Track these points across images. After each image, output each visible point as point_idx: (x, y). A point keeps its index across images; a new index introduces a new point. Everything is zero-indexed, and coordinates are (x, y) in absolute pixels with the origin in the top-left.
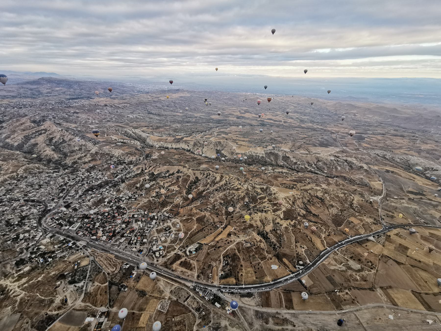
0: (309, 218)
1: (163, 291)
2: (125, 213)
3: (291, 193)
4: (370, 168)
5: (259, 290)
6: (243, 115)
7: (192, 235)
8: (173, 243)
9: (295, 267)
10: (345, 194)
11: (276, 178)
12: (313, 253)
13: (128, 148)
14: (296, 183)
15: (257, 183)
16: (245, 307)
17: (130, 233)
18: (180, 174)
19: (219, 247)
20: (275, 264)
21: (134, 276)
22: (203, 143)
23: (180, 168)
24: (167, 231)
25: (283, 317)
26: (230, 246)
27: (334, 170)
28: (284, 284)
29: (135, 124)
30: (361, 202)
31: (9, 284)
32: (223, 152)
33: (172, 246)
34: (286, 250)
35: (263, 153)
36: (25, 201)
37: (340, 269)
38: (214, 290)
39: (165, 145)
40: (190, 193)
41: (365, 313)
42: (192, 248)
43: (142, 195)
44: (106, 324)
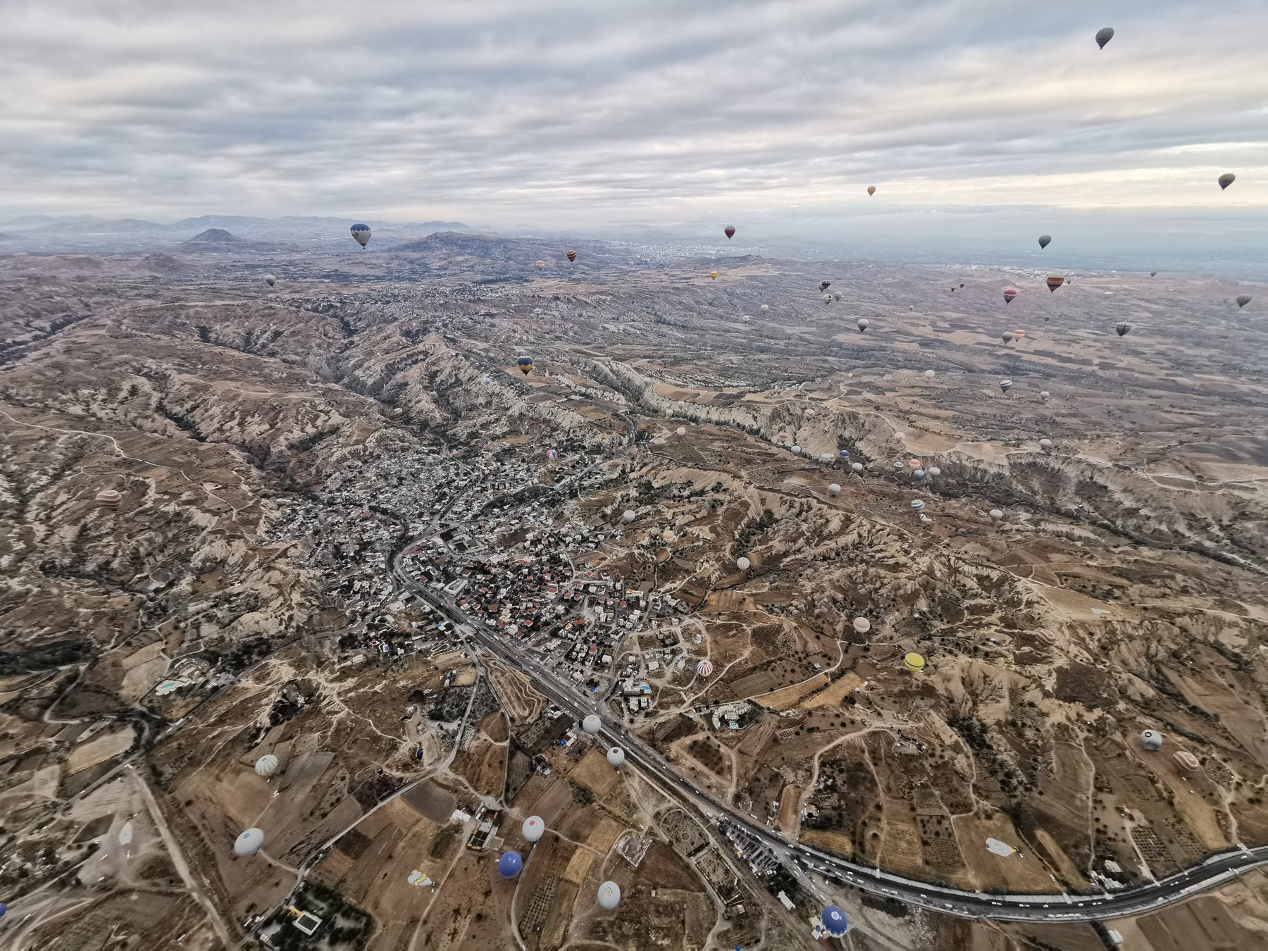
0: (1169, 717)
1: (635, 807)
2: (569, 578)
3: (1098, 612)
5: (930, 902)
6: (943, 336)
7: (738, 675)
8: (680, 684)
9: (1086, 876)
11: (1042, 550)
12: (1174, 849)
13: (594, 410)
14: (1125, 582)
15: (966, 556)
16: (875, 941)
17: (574, 630)
18: (721, 496)
19: (811, 730)
20: (1005, 840)
21: (569, 743)
22: (799, 412)
23: (725, 477)
24: (666, 646)
28: (1033, 918)
29: (619, 349)
31: (322, 681)
32: (860, 445)
33: (676, 692)
34: (1054, 803)
35: (1005, 462)
36: (371, 508)
38: (781, 855)
39: (691, 411)
40: (744, 555)
42: (731, 710)
43: (614, 536)
44: (493, 841)
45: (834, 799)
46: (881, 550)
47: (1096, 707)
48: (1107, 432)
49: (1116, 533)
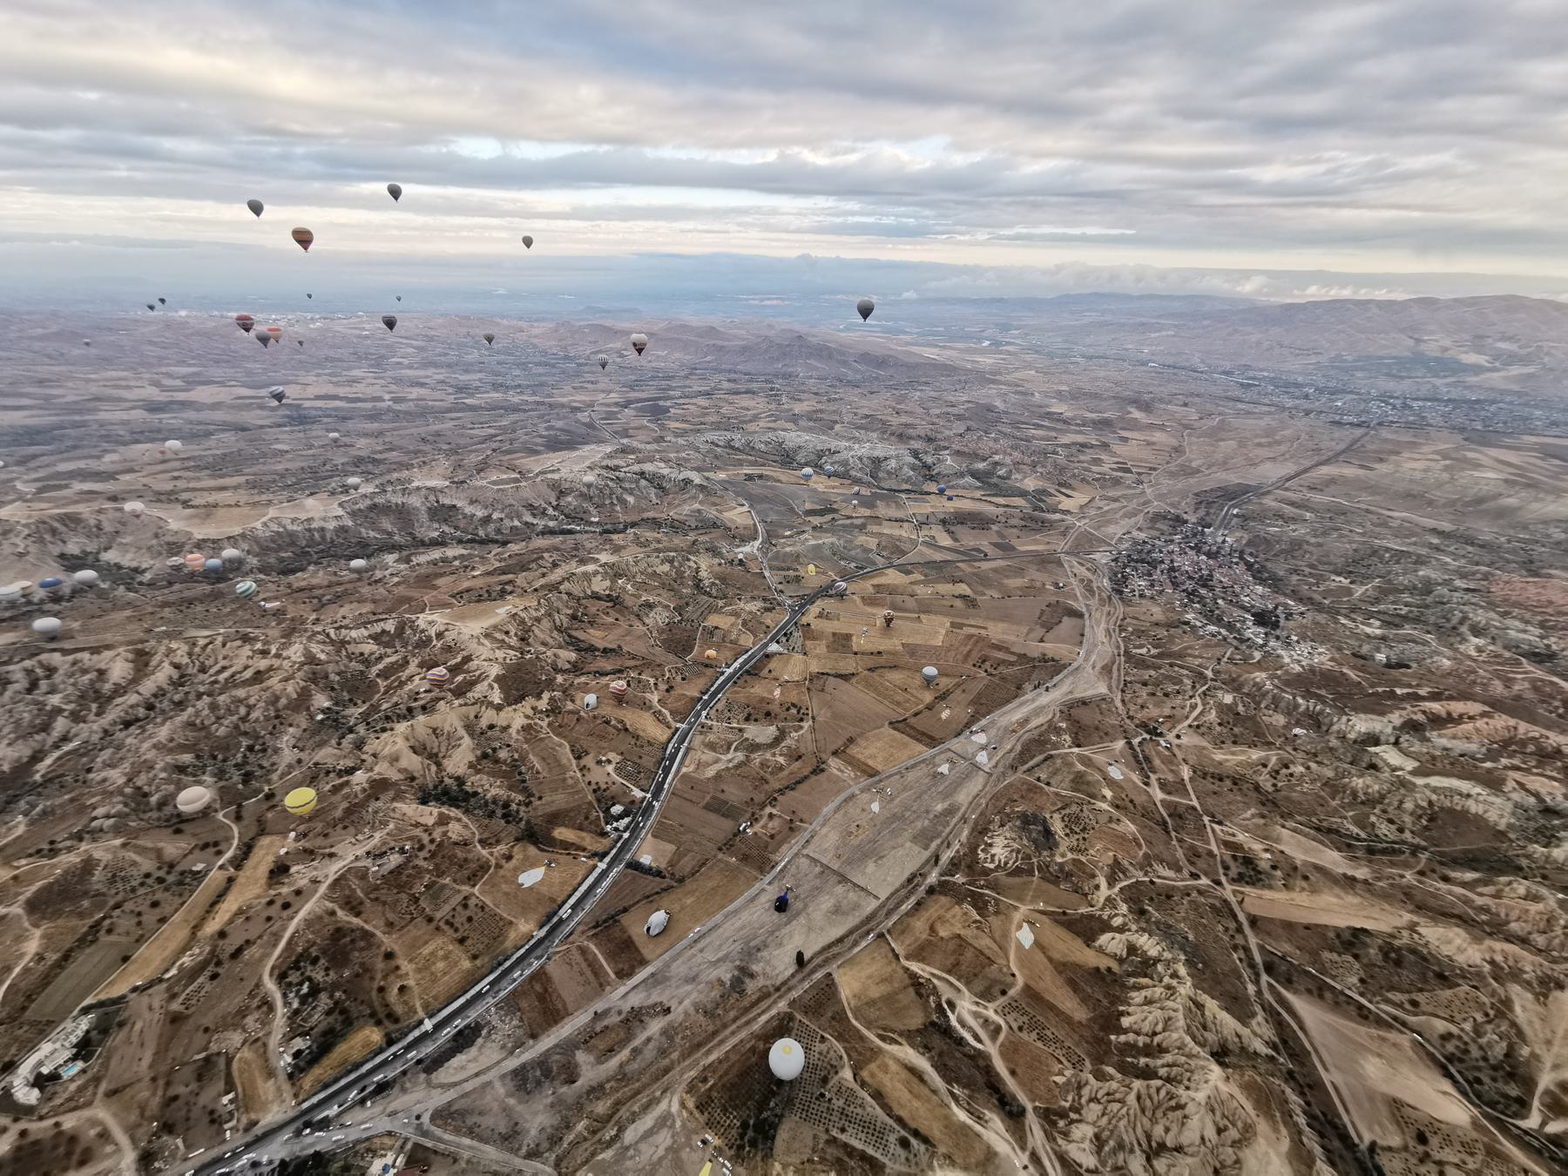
0: (593, 667)
3: (502, 611)
4: (707, 479)
5: (497, 992)
6: (181, 396)
10: (671, 561)
11: (426, 581)
14: (510, 576)
19: (236, 954)
20: (533, 865)
25: (620, 1013)
26: (302, 914)
27: (618, 508)
28: (587, 907)
30: (717, 569)
34: (554, 797)
35: (340, 512)
37: (730, 765)
41: (826, 835)
45: (324, 1001)
46: (224, 668)
47: (542, 692)
48: (430, 457)
49: (482, 542)
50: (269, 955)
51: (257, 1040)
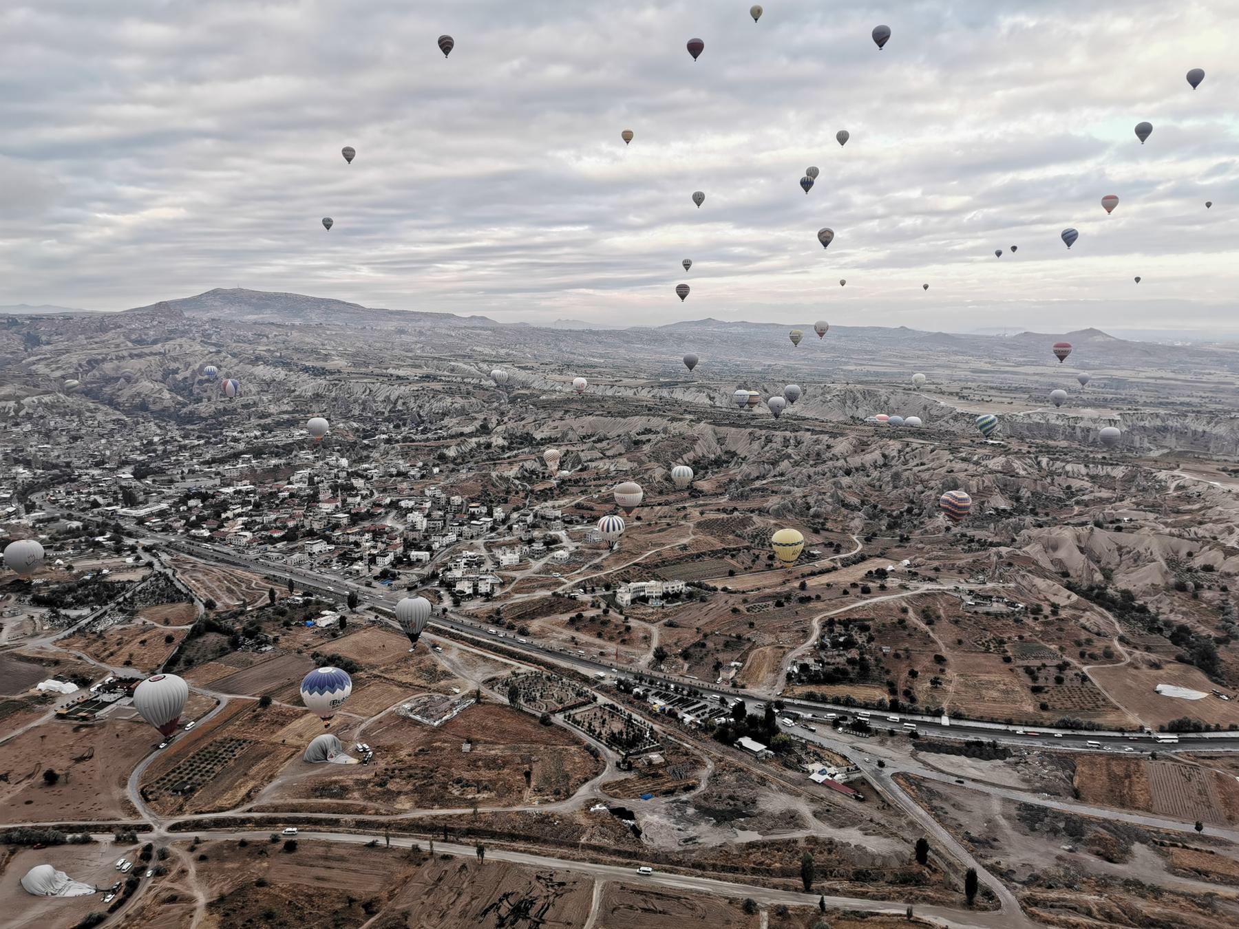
26: (874, 600)
45: (854, 653)
46: (922, 464)
50: (828, 611)
51: (782, 647)
